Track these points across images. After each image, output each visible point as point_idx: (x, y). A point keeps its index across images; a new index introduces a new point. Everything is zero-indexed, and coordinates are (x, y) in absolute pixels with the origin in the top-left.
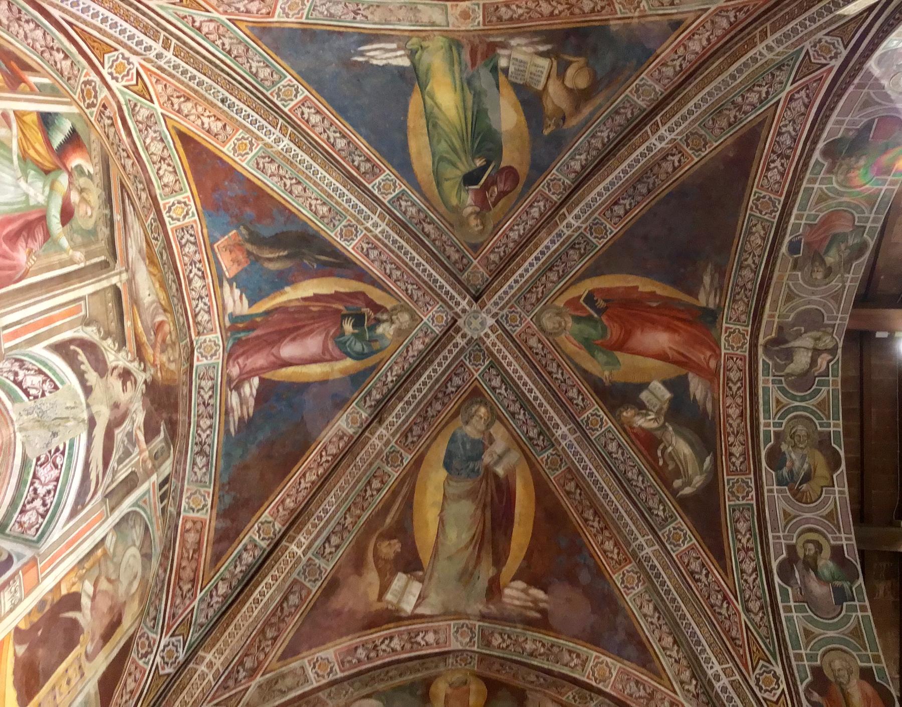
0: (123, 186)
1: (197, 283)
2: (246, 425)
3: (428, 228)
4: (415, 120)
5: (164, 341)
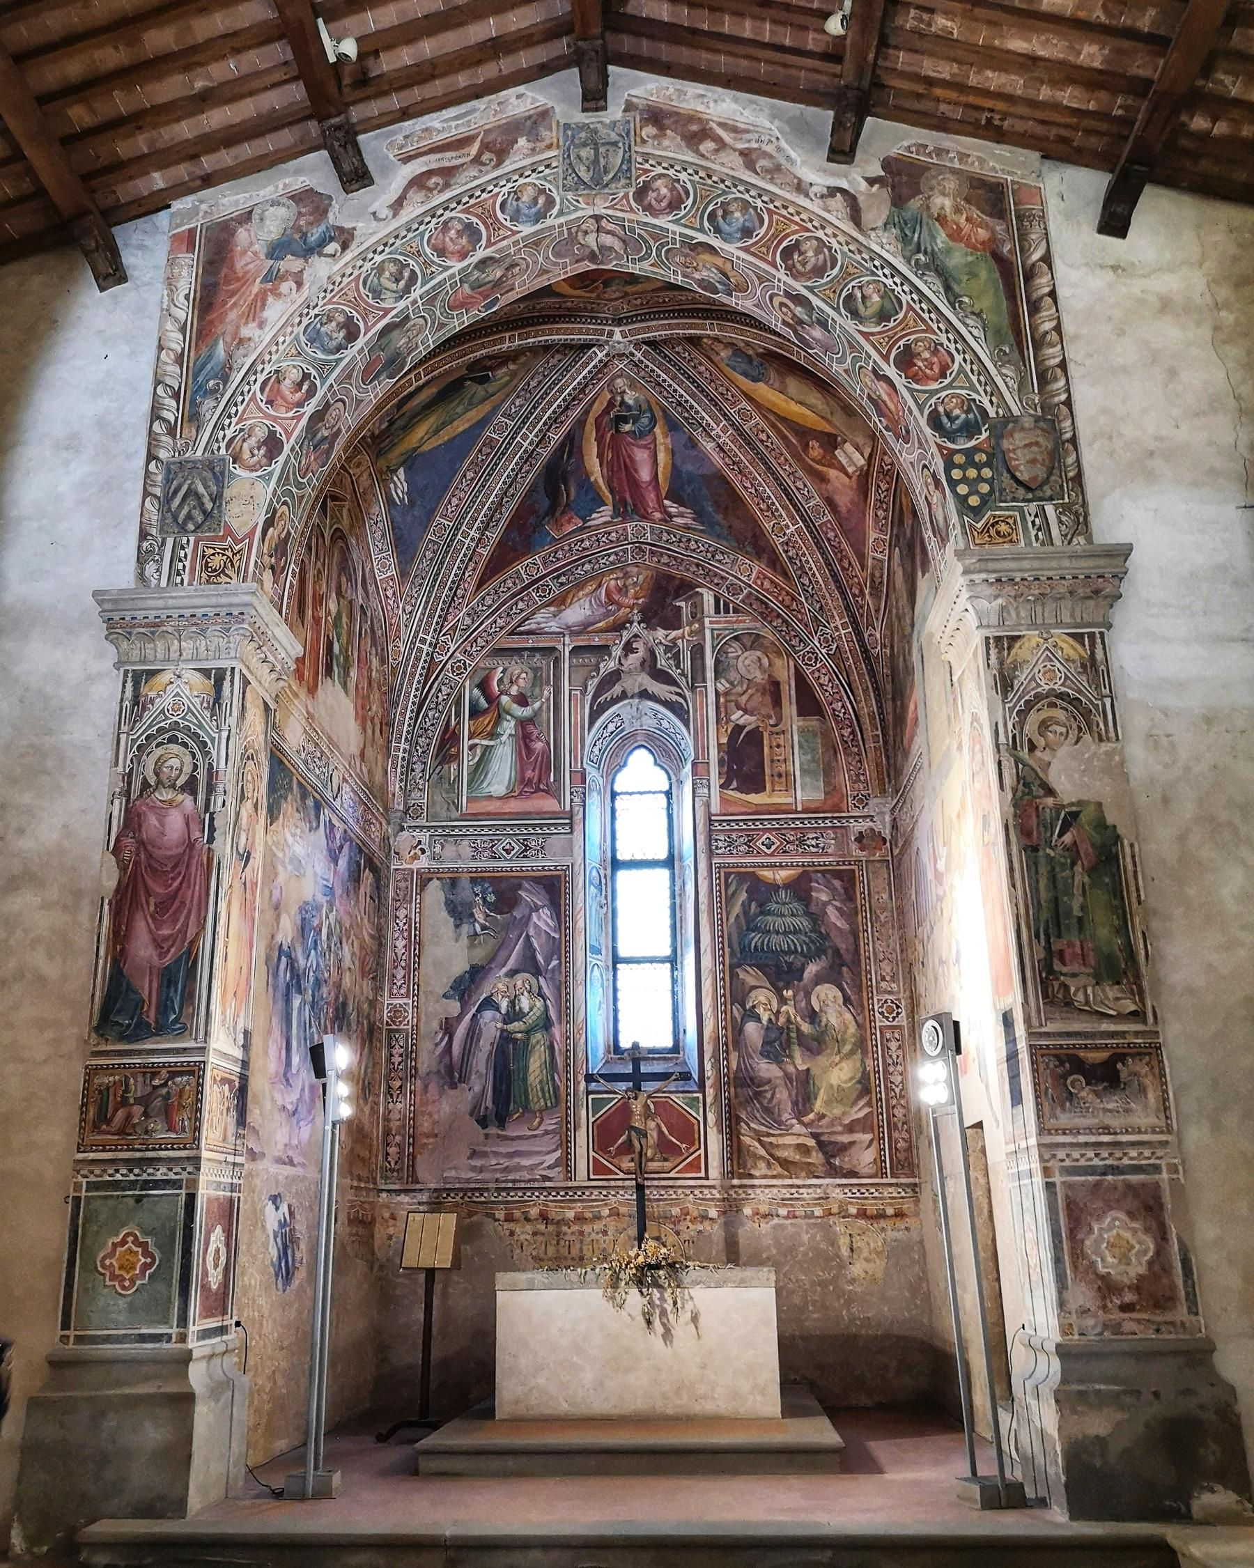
0: (512, 633)
1: (587, 543)
2: (699, 516)
3: (533, 384)
4: (444, 437)
5: (619, 590)
